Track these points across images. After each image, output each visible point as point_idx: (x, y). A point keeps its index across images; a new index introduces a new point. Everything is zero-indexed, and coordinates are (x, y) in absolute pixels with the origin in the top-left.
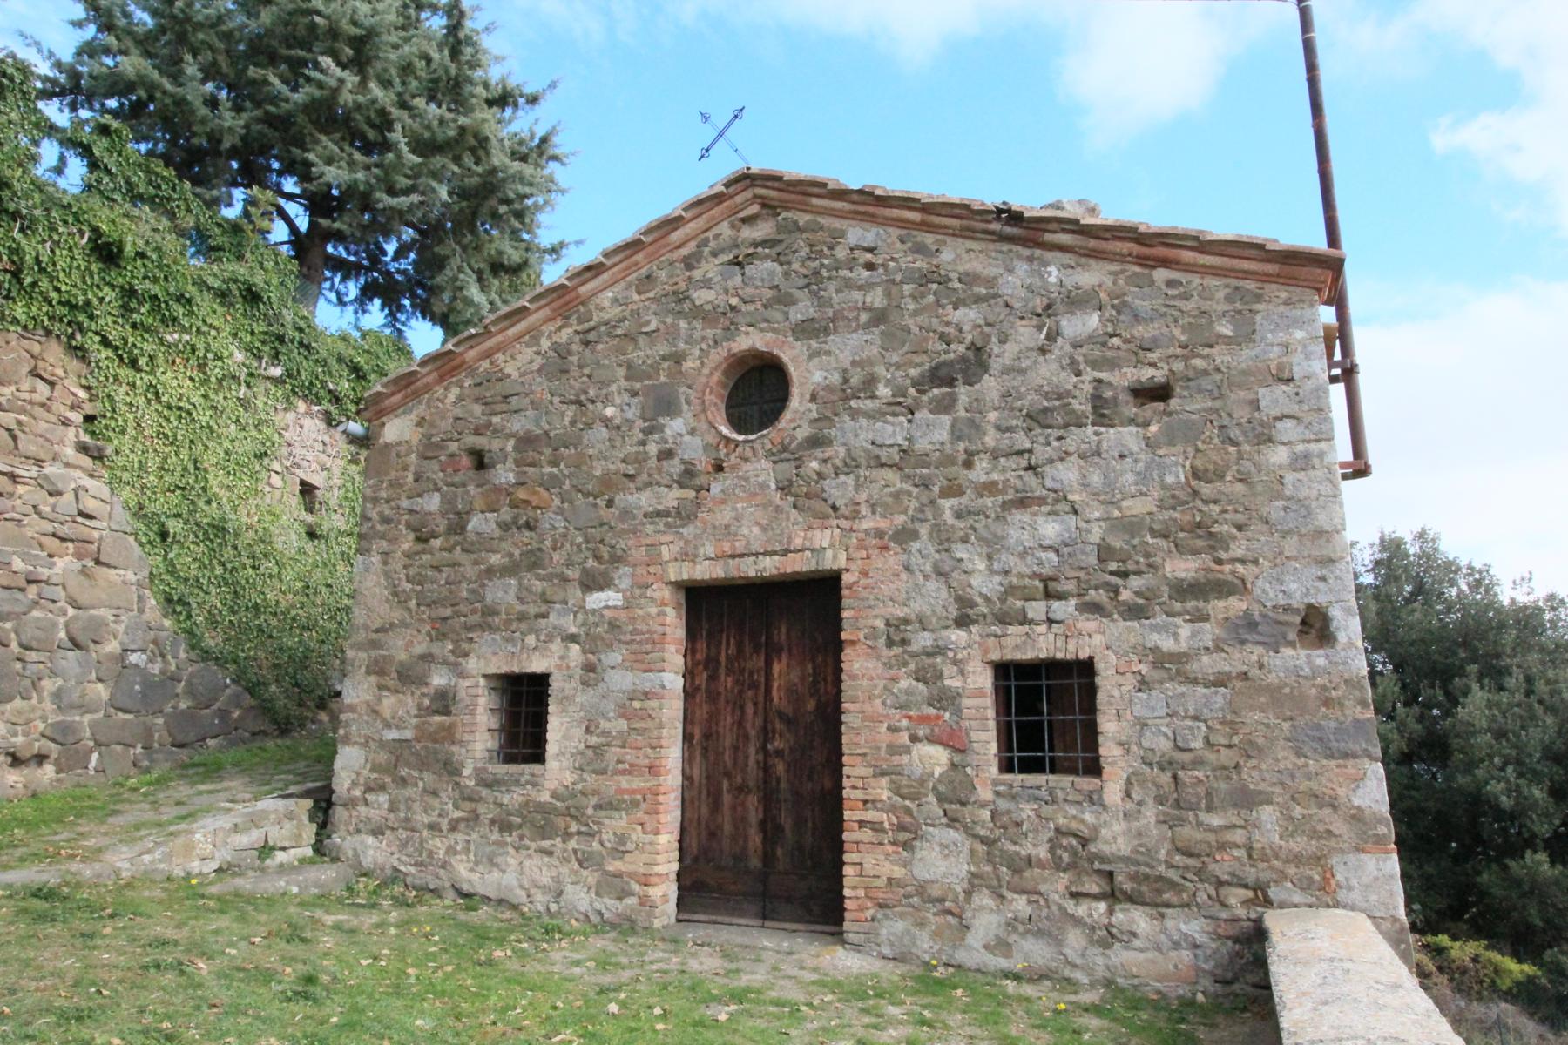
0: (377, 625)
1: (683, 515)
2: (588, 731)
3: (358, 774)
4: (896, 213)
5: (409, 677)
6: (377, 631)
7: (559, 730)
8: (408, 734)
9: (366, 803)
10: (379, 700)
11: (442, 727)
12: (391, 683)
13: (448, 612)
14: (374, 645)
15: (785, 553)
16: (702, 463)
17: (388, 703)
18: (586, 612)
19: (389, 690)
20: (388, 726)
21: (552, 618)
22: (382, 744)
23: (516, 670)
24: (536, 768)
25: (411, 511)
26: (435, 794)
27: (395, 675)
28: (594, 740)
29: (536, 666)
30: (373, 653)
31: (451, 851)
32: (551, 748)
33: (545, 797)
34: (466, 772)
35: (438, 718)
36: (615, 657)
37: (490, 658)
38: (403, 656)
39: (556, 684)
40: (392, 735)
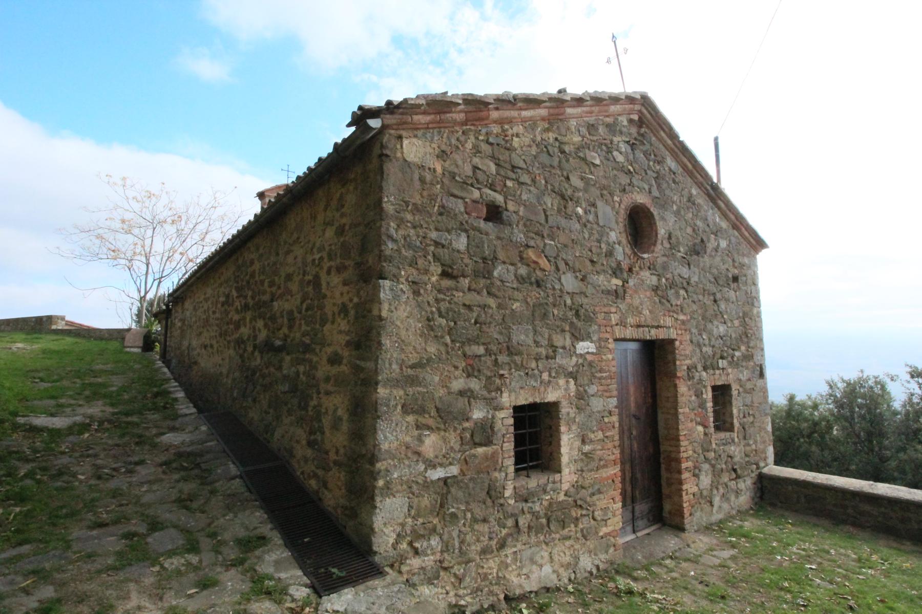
0: (413, 358)
1: (618, 295)
2: (583, 442)
3: (403, 525)
4: (685, 160)
5: (446, 416)
6: (413, 367)
7: (568, 445)
8: (454, 470)
9: (416, 552)
10: (420, 439)
11: (486, 457)
12: (431, 422)
13: (481, 350)
14: (413, 381)
15: (658, 327)
16: (625, 266)
17: (431, 444)
18: (577, 355)
19: (429, 428)
20: (431, 465)
21: (559, 360)
22: (427, 485)
23: (538, 400)
24: (557, 477)
25: (437, 244)
26: (485, 520)
27: (433, 412)
28: (587, 448)
29: (551, 397)
30: (410, 391)
31: (504, 565)
32: (565, 459)
33: (562, 497)
34: (508, 493)
35: (480, 450)
36: (592, 389)
37: (514, 396)
38: (442, 392)
39: (566, 410)
40: (438, 474)
